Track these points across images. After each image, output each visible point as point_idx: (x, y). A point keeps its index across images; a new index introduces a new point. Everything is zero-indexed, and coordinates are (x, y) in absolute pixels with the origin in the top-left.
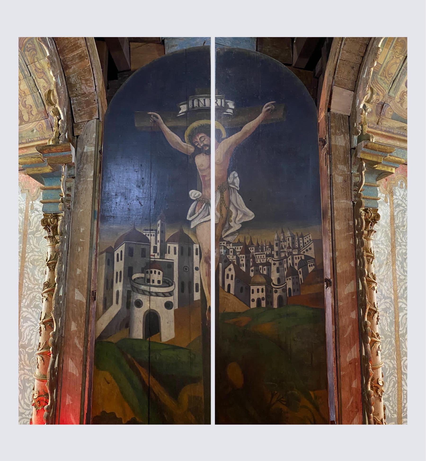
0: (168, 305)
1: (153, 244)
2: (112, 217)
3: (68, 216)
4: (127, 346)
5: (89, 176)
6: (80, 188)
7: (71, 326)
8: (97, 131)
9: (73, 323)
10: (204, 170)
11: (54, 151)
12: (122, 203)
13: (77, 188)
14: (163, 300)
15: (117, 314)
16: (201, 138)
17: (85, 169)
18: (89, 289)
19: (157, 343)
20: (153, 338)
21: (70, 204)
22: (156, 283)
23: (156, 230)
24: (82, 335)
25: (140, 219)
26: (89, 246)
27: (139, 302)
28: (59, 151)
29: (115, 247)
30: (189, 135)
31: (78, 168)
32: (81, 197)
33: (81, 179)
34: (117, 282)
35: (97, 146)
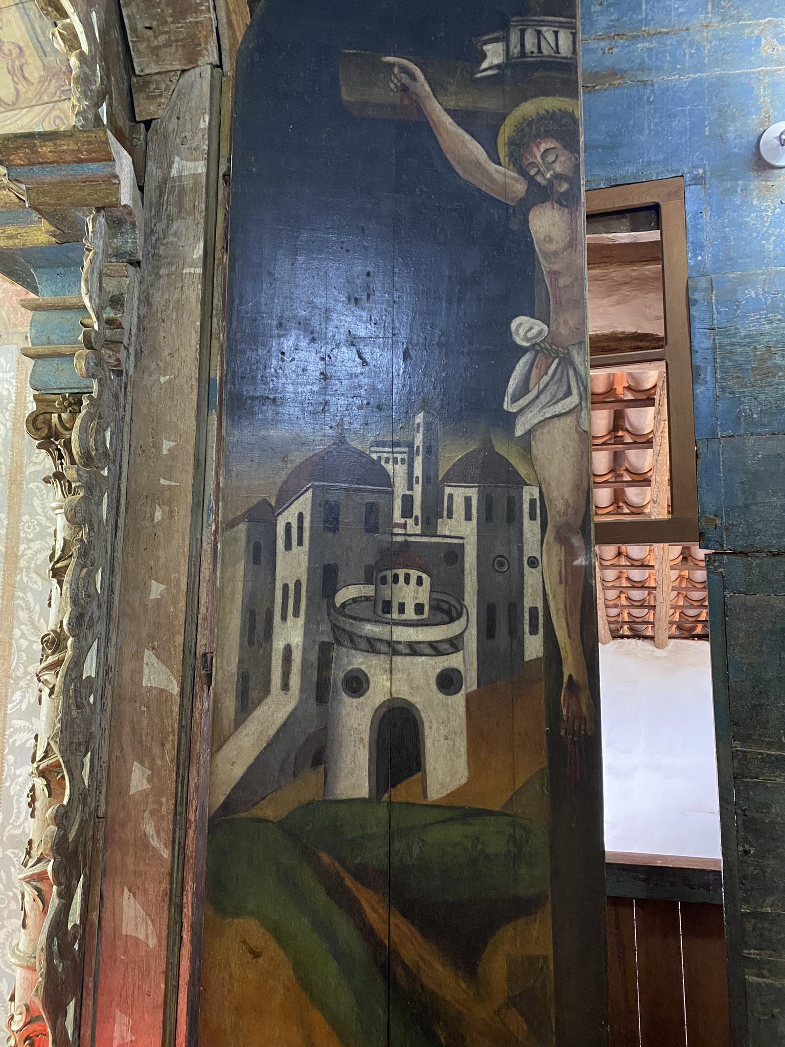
0: (448, 682)
1: (400, 489)
2: (268, 402)
3: (116, 397)
4: (319, 831)
5: (189, 260)
6: (158, 299)
7: (129, 779)
8: (216, 109)
9: (136, 766)
10: (556, 254)
11: (51, 157)
12: (302, 355)
13: (146, 300)
14: (429, 667)
15: (285, 724)
16: (546, 151)
17: (175, 234)
18: (189, 650)
19: (413, 804)
20: (402, 792)
21: (122, 355)
22: (410, 614)
23: (410, 445)
24: (167, 806)
25: (360, 407)
26: (190, 500)
27: (357, 678)
28: (68, 158)
29: (277, 502)
30: (511, 143)
31: (152, 232)
32: (162, 334)
33: (163, 271)
34: (284, 618)
35: (213, 158)
